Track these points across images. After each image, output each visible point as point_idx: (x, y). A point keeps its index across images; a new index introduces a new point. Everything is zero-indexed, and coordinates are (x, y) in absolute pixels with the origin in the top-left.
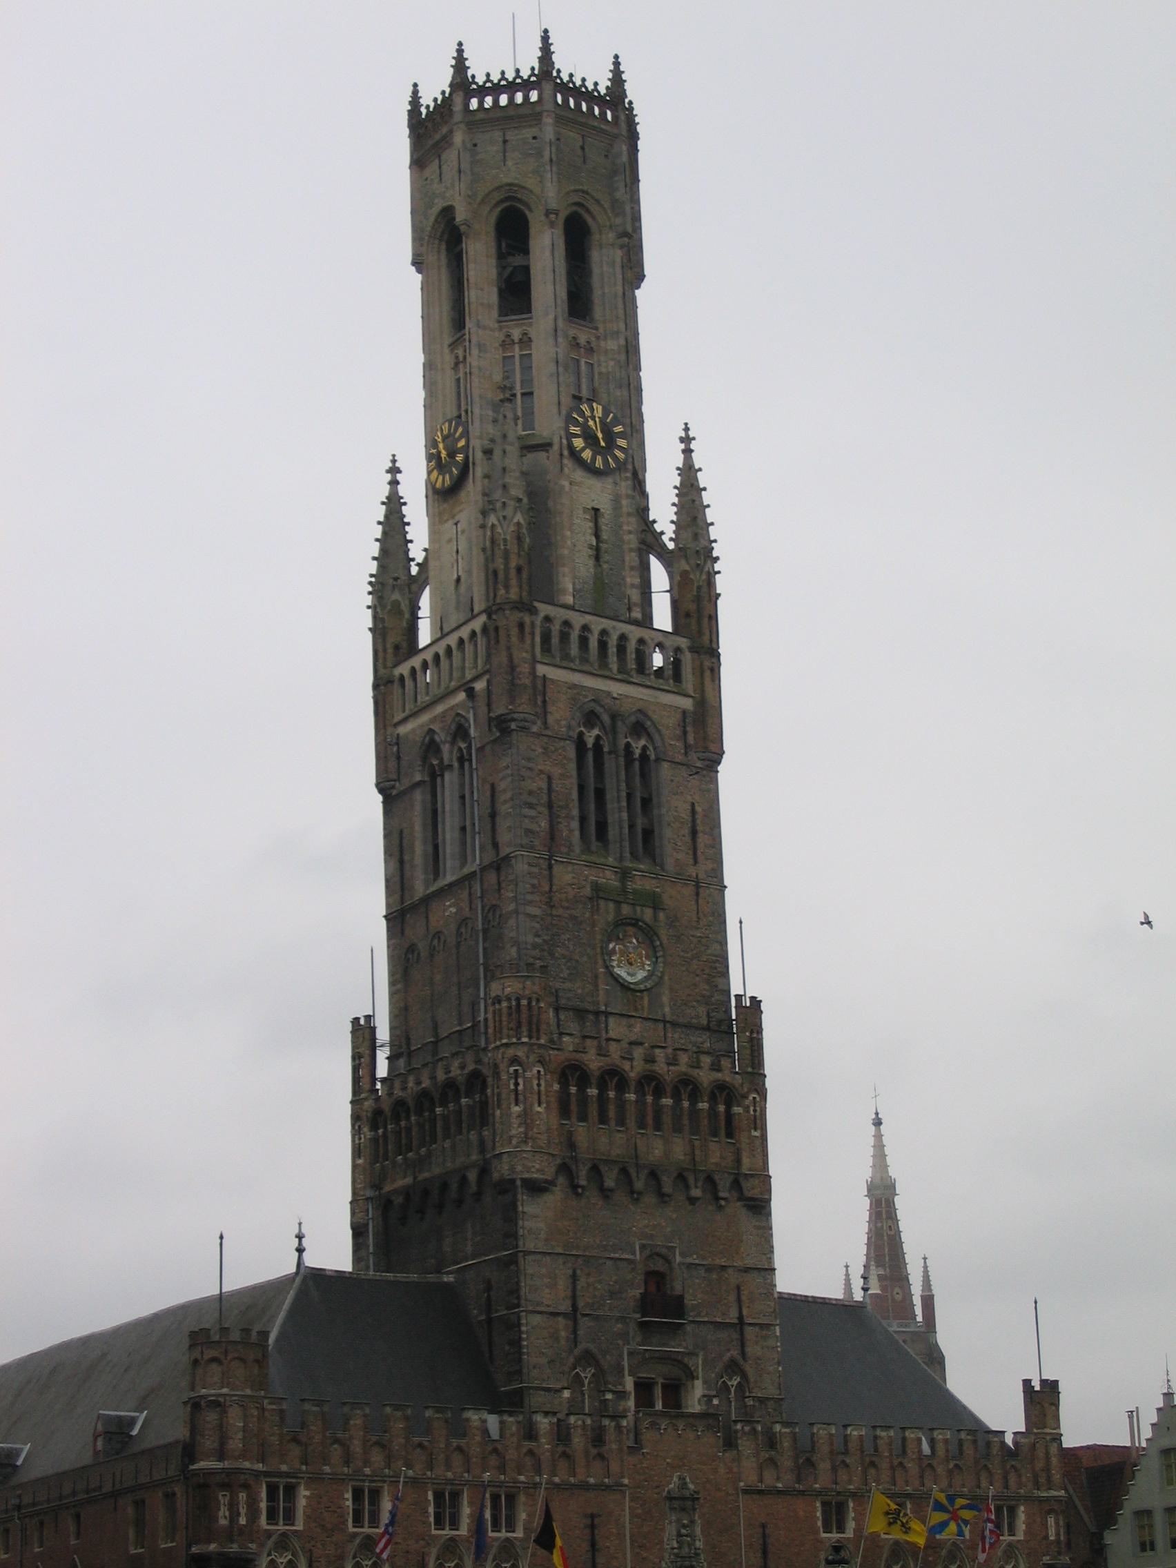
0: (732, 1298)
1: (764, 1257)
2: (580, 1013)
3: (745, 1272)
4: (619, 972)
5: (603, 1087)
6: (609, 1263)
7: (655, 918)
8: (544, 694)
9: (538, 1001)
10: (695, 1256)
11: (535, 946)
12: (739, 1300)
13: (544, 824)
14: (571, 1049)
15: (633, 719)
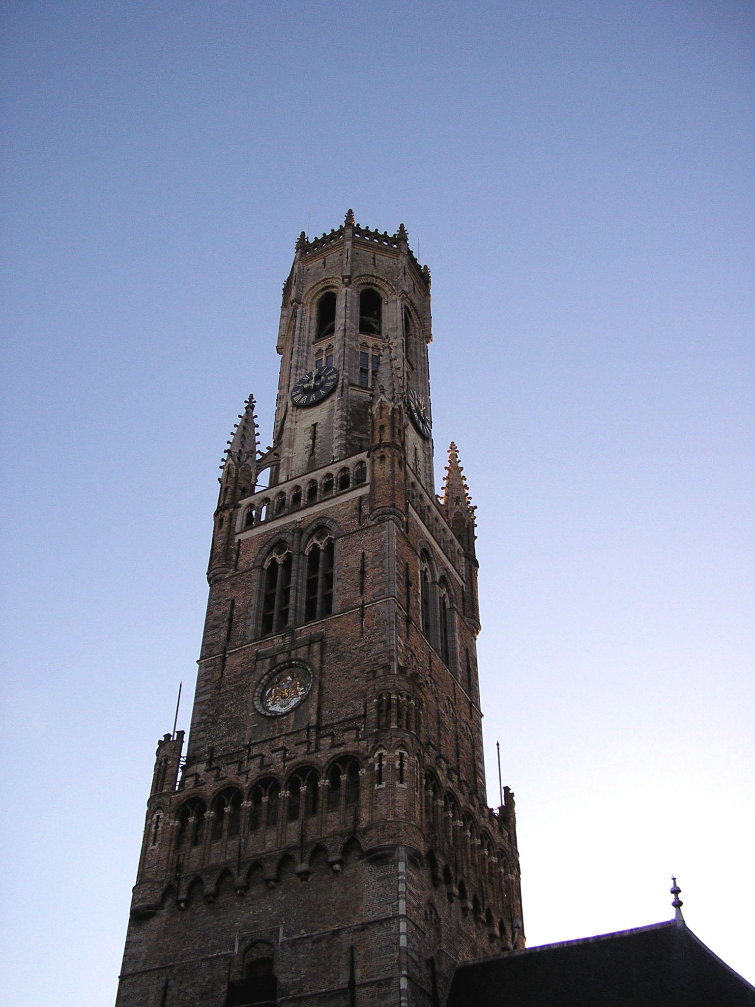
0: (344, 963)
1: (388, 906)
2: (229, 757)
3: (363, 930)
4: (273, 709)
5: (218, 805)
6: (205, 965)
7: (309, 652)
8: (239, 551)
9: (166, 761)
10: (302, 931)
11: (199, 723)
12: (352, 964)
13: (223, 634)
14: (191, 787)
15: (314, 526)
